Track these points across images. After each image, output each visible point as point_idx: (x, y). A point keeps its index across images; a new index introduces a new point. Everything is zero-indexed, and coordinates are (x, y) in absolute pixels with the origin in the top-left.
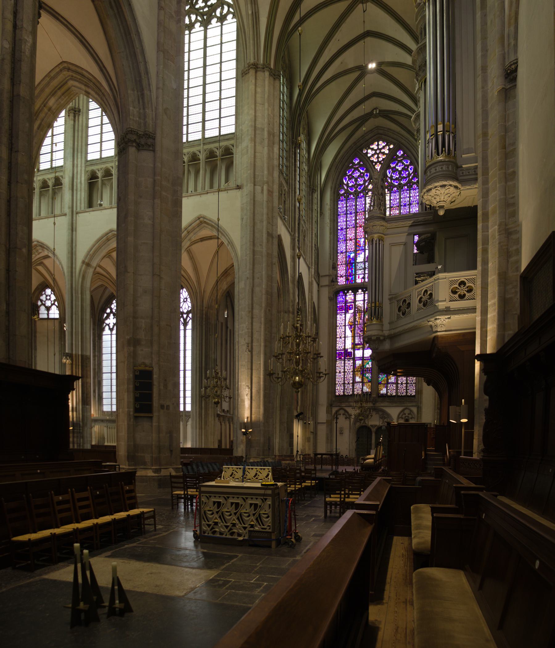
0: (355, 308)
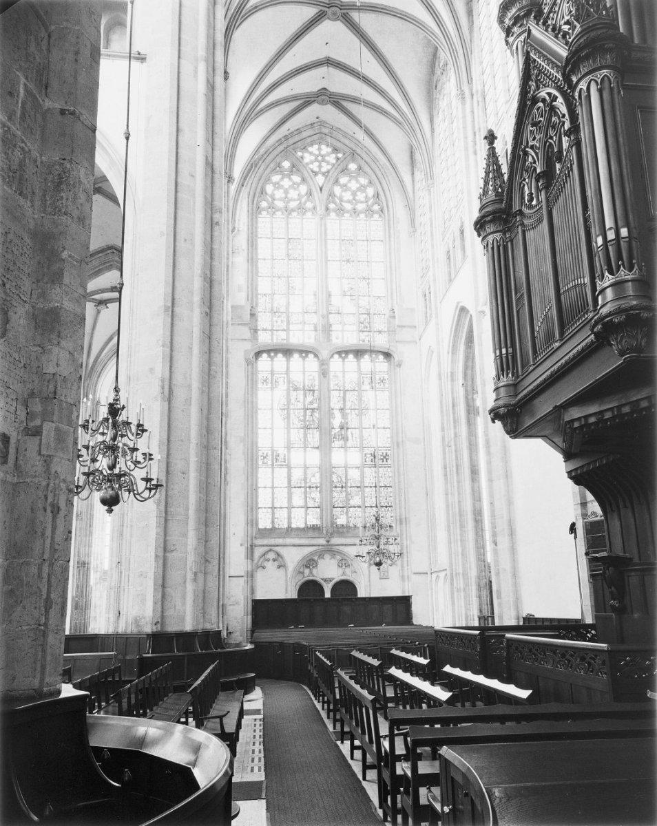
0: (289, 382)
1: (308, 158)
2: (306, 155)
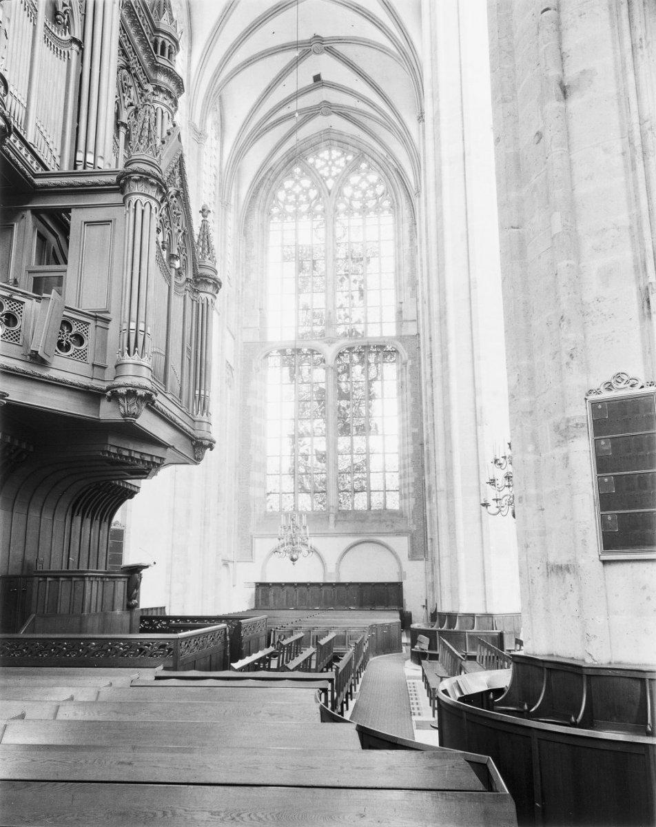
1: (319, 164)
2: (318, 161)
